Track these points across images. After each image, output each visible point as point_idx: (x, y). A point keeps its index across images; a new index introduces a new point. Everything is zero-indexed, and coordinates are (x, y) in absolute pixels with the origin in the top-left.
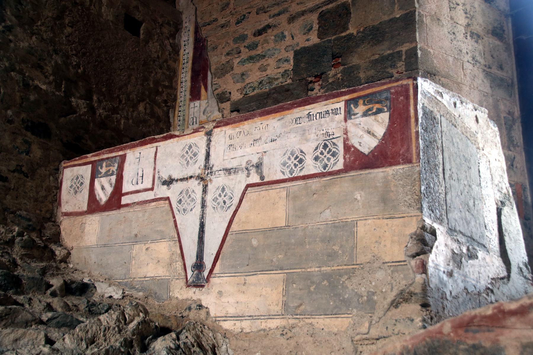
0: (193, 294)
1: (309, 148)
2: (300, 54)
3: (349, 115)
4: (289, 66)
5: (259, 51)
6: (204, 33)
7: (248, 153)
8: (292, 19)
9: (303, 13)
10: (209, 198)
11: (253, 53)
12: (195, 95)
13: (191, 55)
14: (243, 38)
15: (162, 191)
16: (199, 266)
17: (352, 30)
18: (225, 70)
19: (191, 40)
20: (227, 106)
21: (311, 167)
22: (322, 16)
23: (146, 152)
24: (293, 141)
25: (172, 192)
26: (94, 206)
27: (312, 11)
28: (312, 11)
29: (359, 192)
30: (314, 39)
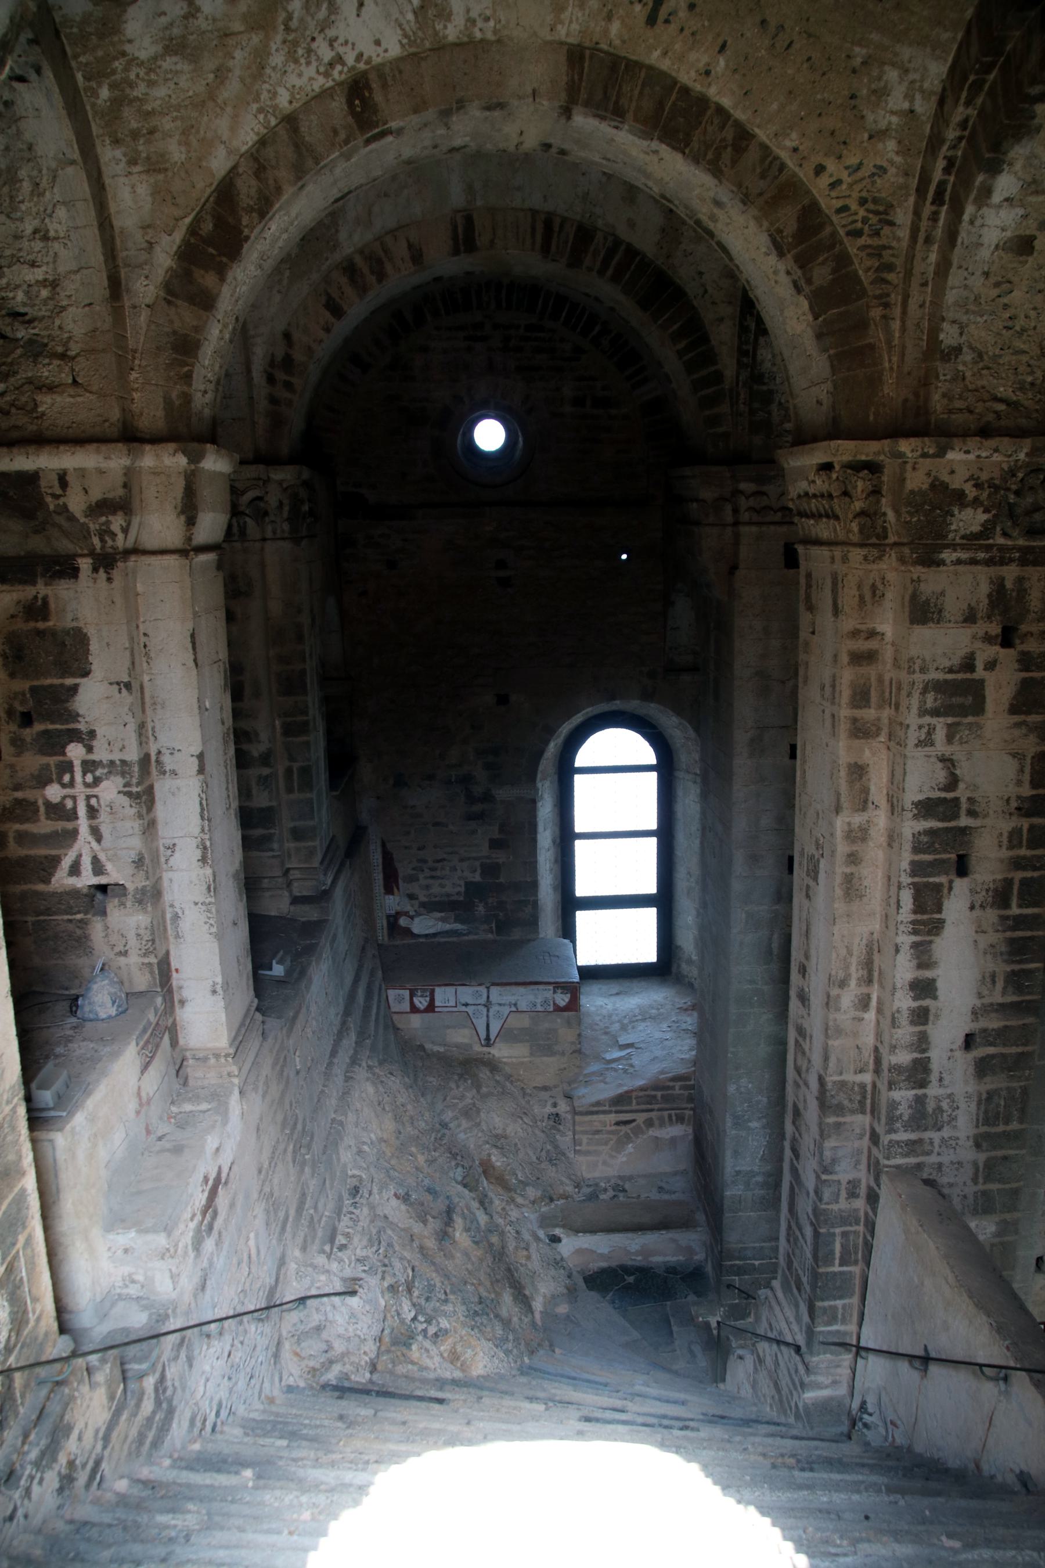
0: (485, 1049)
1: (539, 1001)
2: (468, 884)
3: (555, 992)
4: (462, 889)
5: (438, 873)
6: (389, 846)
7: (512, 999)
8: (462, 860)
9: (469, 859)
10: (491, 1014)
11: (434, 873)
12: (389, 890)
13: (380, 861)
14: (425, 861)
15: (464, 1009)
16: (488, 1038)
17: (502, 880)
18: (411, 879)
19: (379, 850)
20: (416, 903)
21: (539, 1008)
22: (482, 865)
23: (450, 990)
24: (531, 998)
25: (470, 1010)
26: (414, 1009)
27: (475, 859)
28: (475, 859)
29: (559, 1019)
30: (477, 878)
